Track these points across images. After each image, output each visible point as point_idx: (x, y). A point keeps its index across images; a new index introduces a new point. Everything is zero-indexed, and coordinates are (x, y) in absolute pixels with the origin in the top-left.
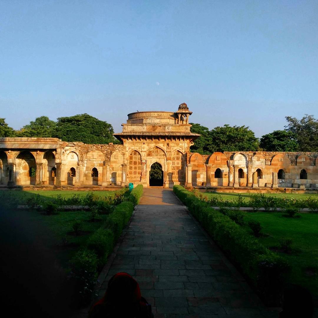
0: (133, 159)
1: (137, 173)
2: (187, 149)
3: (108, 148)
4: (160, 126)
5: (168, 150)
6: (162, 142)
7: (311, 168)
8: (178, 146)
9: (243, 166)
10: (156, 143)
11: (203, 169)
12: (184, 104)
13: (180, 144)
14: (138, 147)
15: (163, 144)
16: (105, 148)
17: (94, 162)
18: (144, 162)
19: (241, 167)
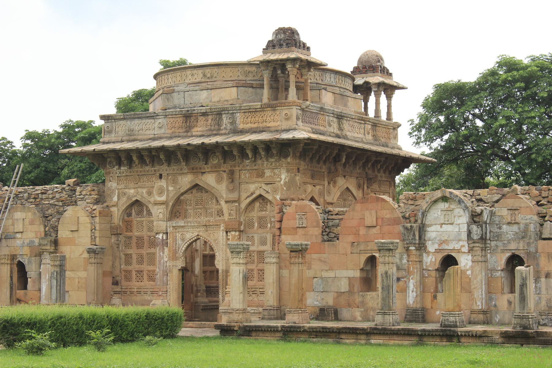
0: (135, 230)
1: (145, 277)
3: (57, 196)
4: (204, 114)
6: (211, 167)
8: (260, 179)
9: (457, 247)
10: (194, 171)
11: (320, 260)
12: (281, 31)
13: (268, 173)
14: (144, 191)
15: (214, 175)
16: (51, 196)
19: (453, 250)
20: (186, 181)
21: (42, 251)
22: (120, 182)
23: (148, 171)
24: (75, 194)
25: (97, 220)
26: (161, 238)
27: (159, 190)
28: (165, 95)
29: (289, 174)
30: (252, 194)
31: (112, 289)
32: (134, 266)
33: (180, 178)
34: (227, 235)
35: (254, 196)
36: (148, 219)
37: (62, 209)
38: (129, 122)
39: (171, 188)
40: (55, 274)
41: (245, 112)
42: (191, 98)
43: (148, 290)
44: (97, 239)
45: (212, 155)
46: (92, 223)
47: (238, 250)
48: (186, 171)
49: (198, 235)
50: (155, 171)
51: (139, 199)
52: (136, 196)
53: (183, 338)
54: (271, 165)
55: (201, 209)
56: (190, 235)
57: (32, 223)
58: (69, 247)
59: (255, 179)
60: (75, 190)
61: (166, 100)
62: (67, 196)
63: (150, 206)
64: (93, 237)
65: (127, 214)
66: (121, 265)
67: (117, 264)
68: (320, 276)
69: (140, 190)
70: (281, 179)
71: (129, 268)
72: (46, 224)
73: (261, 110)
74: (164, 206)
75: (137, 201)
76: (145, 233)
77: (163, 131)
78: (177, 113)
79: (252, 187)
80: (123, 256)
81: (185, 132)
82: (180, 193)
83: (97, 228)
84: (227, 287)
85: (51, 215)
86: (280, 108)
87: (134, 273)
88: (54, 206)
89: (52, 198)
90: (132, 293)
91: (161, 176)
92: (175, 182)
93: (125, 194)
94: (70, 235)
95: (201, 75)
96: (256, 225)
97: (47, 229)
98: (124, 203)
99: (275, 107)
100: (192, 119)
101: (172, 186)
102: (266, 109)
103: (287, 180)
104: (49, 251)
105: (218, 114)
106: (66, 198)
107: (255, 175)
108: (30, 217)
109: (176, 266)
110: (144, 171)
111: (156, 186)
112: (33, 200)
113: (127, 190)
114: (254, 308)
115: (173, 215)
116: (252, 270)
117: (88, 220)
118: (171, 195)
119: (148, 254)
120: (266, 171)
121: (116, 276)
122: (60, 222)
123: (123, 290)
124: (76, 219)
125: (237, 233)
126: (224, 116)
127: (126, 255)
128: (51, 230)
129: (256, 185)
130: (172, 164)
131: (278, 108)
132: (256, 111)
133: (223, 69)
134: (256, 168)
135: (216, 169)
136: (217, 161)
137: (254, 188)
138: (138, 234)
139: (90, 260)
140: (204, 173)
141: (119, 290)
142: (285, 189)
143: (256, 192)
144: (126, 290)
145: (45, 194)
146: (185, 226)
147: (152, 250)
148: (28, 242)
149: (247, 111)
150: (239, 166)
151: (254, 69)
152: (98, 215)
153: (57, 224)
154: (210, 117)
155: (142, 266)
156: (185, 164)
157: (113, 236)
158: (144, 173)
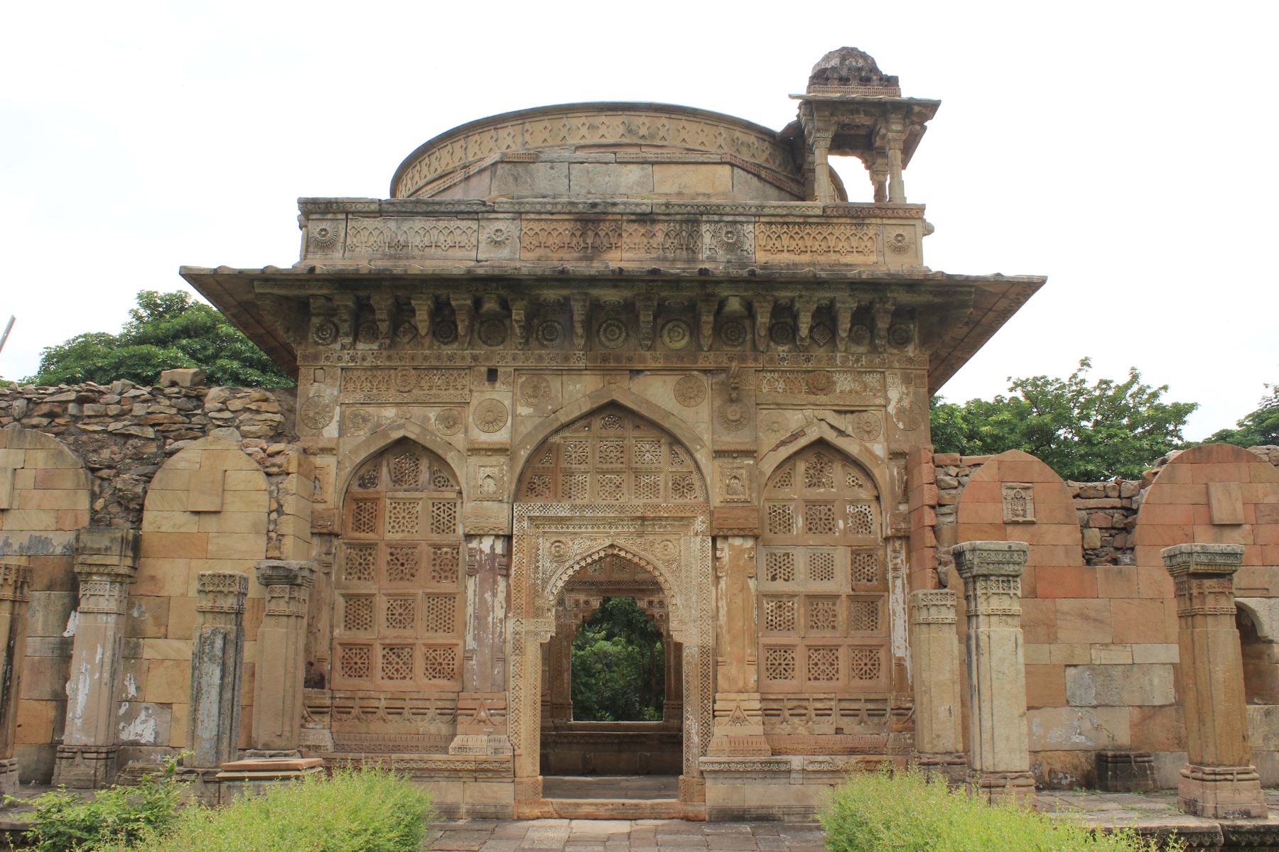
1: (419, 665)
2: (911, 427)
3: (139, 409)
4: (645, 218)
5: (731, 440)
6: (667, 358)
8: (822, 398)
10: (606, 366)
11: (1086, 618)
12: (847, 54)
13: (844, 383)
14: (432, 414)
15: (671, 380)
16: (113, 410)
18: (493, 555)
20: (579, 391)
21: (86, 569)
22: (350, 386)
23: (451, 358)
24: (202, 406)
25: (291, 483)
26: (487, 550)
27: (489, 414)
28: (508, 167)
29: (911, 389)
30: (794, 437)
31: (306, 697)
32: (380, 632)
33: (555, 383)
34: (714, 548)
35: (803, 442)
36: (435, 495)
37: (152, 448)
38: (392, 224)
39: (524, 410)
40: (219, 643)
41: (770, 223)
42: (591, 181)
43: (427, 704)
44: (288, 543)
45: (670, 325)
46: (271, 493)
47: (1010, 569)
48: (581, 365)
49: (612, 546)
50: (475, 358)
51: (412, 436)
52: (400, 427)
54: (857, 361)
55: (618, 473)
57: (45, 482)
58: (181, 563)
59: (803, 398)
60: (200, 398)
61: (511, 179)
62: (174, 411)
63: (451, 457)
64: (273, 535)
65: (362, 478)
66: (332, 627)
67: (323, 624)
68: (1086, 660)
69: (416, 411)
70: (888, 400)
71: (362, 636)
72: (97, 489)
73: (823, 220)
74: (502, 459)
75: (404, 441)
76: (421, 533)
77: (505, 253)
78: (559, 207)
79: (794, 419)
80: (341, 603)
81: (580, 259)
82: (556, 425)
83: (286, 509)
84: (718, 696)
85: (110, 467)
86: (879, 221)
87: (378, 652)
88: (120, 441)
89: (117, 417)
90: (368, 712)
91: (492, 375)
92: (535, 393)
93: (365, 420)
94: (191, 525)
95: (621, 130)
96: (800, 521)
97: (99, 504)
98: (359, 445)
99: (864, 218)
100: (604, 227)
101: (528, 405)
102: (835, 220)
103: (906, 403)
104: (117, 570)
105: (686, 222)
106: (172, 416)
107: (804, 388)
108: (41, 465)
109: (537, 634)
110: (439, 358)
111: (475, 402)
112: (45, 421)
113: (371, 410)
114: (821, 758)
115: (525, 486)
116: (787, 648)
117: (260, 480)
118: (524, 430)
119: (429, 596)
120: (836, 377)
121: (321, 660)
122: (155, 482)
123: (337, 702)
124: (220, 475)
125: (749, 543)
126: (704, 228)
127: (348, 597)
128: (114, 509)
129: (808, 413)
130: (533, 343)
131: (874, 221)
132: (805, 221)
133: (684, 123)
134: (810, 366)
135: (678, 367)
136: (684, 342)
137: (804, 420)
138: (399, 536)
139: (273, 606)
140: (639, 372)
141: (328, 702)
142: (901, 425)
143: (808, 431)
144: (349, 703)
145: (93, 401)
146: (570, 519)
147: (446, 586)
148: (26, 541)
149: (781, 220)
150: (756, 360)
151: (752, 139)
152: (293, 468)
153: (139, 489)
154: (660, 230)
155: (408, 632)
156: (582, 342)
157: (316, 541)
158: (434, 363)
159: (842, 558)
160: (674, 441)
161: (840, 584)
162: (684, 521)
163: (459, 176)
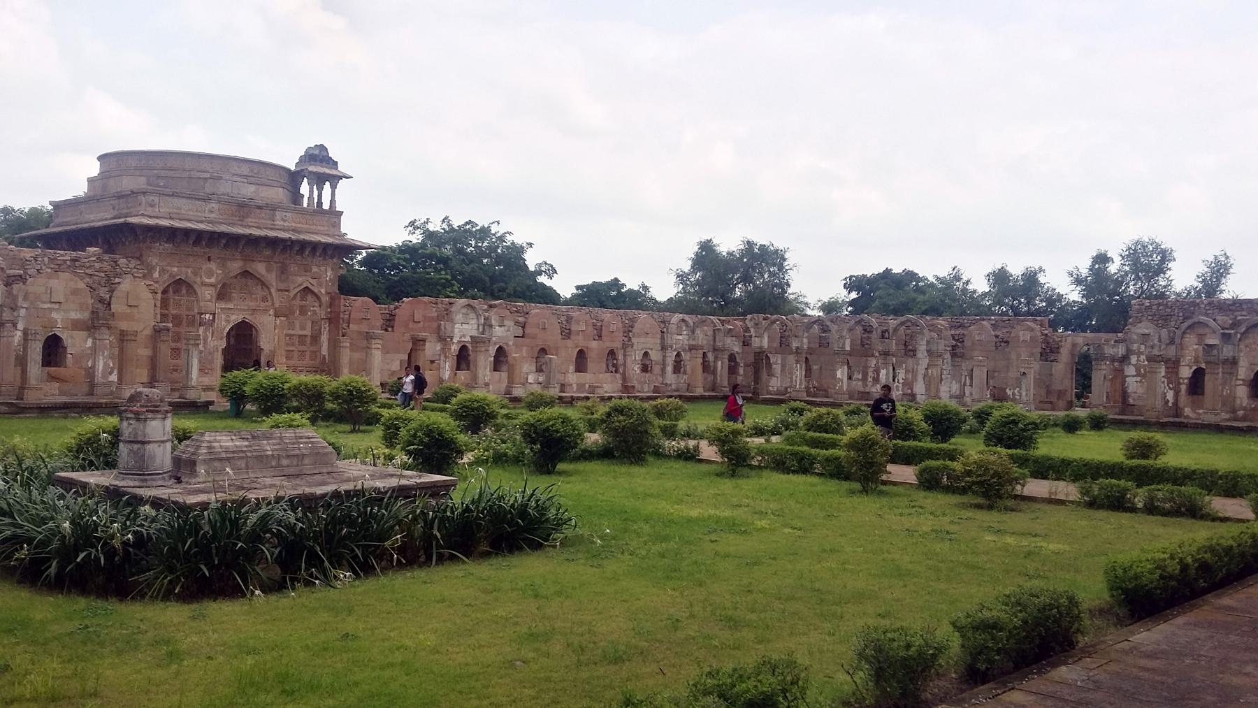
5: (282, 286)
7: (594, 344)
10: (246, 259)
13: (315, 269)
17: (54, 315)
20: (236, 266)
27: (208, 274)
53: (213, 412)
56: (236, 318)
69: (184, 269)
76: (183, 312)
77: (213, 215)
79: (300, 279)
92: (223, 265)
135: (268, 260)
137: (302, 280)
159: (309, 324)
160: (263, 284)
161: (308, 332)
162: (266, 311)
163: (186, 174)
